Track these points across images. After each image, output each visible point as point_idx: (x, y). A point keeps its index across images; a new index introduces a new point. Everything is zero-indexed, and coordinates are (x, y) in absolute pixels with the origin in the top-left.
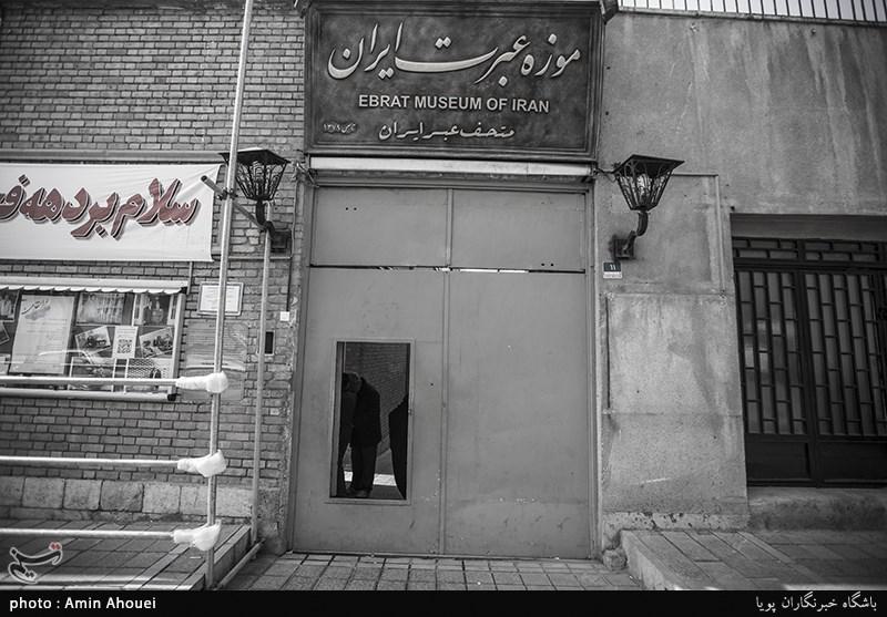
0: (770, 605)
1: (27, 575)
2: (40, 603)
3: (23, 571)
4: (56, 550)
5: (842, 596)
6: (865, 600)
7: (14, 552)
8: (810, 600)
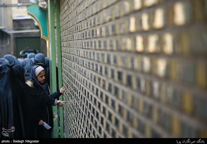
0: (180, 142)
1: (6, 134)
2: (8, 141)
3: (5, 133)
4: (13, 128)
5: (196, 139)
6: (202, 141)
7: (3, 129)
8: (189, 141)
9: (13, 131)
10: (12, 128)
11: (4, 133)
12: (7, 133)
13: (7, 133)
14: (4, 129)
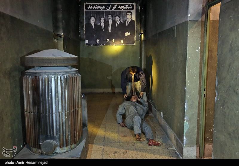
1: (7, 155)
3: (6, 154)
4: (15, 148)
7: (4, 148)
9: (15, 151)
10: (13, 147)
11: (4, 154)
12: (8, 153)
13: (8, 153)
14: (5, 148)
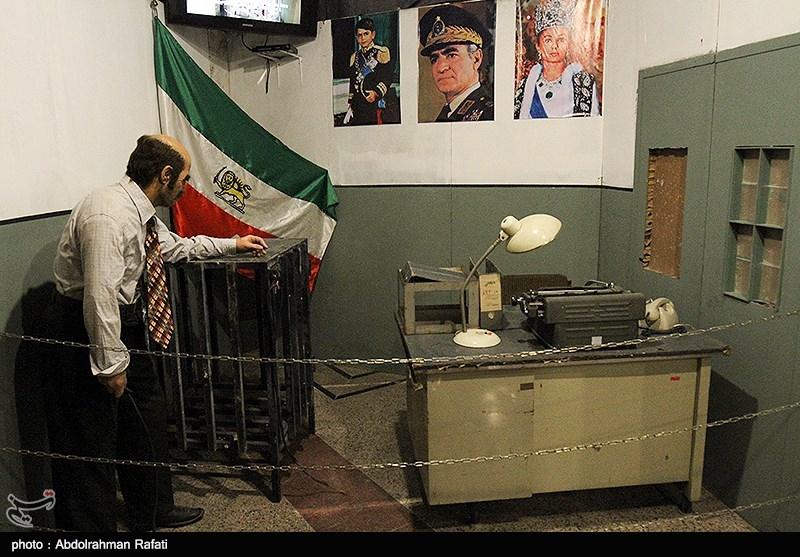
1: (24, 519)
2: (35, 545)
3: (20, 515)
4: (49, 497)
7: (11, 498)
9: (49, 506)
11: (13, 516)
12: (25, 513)
